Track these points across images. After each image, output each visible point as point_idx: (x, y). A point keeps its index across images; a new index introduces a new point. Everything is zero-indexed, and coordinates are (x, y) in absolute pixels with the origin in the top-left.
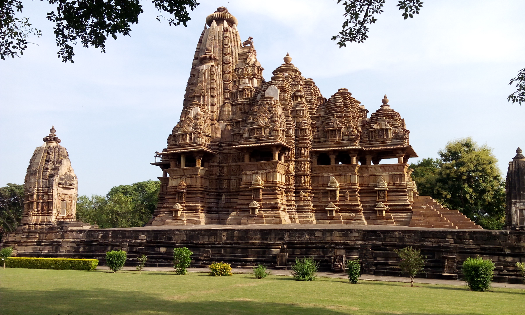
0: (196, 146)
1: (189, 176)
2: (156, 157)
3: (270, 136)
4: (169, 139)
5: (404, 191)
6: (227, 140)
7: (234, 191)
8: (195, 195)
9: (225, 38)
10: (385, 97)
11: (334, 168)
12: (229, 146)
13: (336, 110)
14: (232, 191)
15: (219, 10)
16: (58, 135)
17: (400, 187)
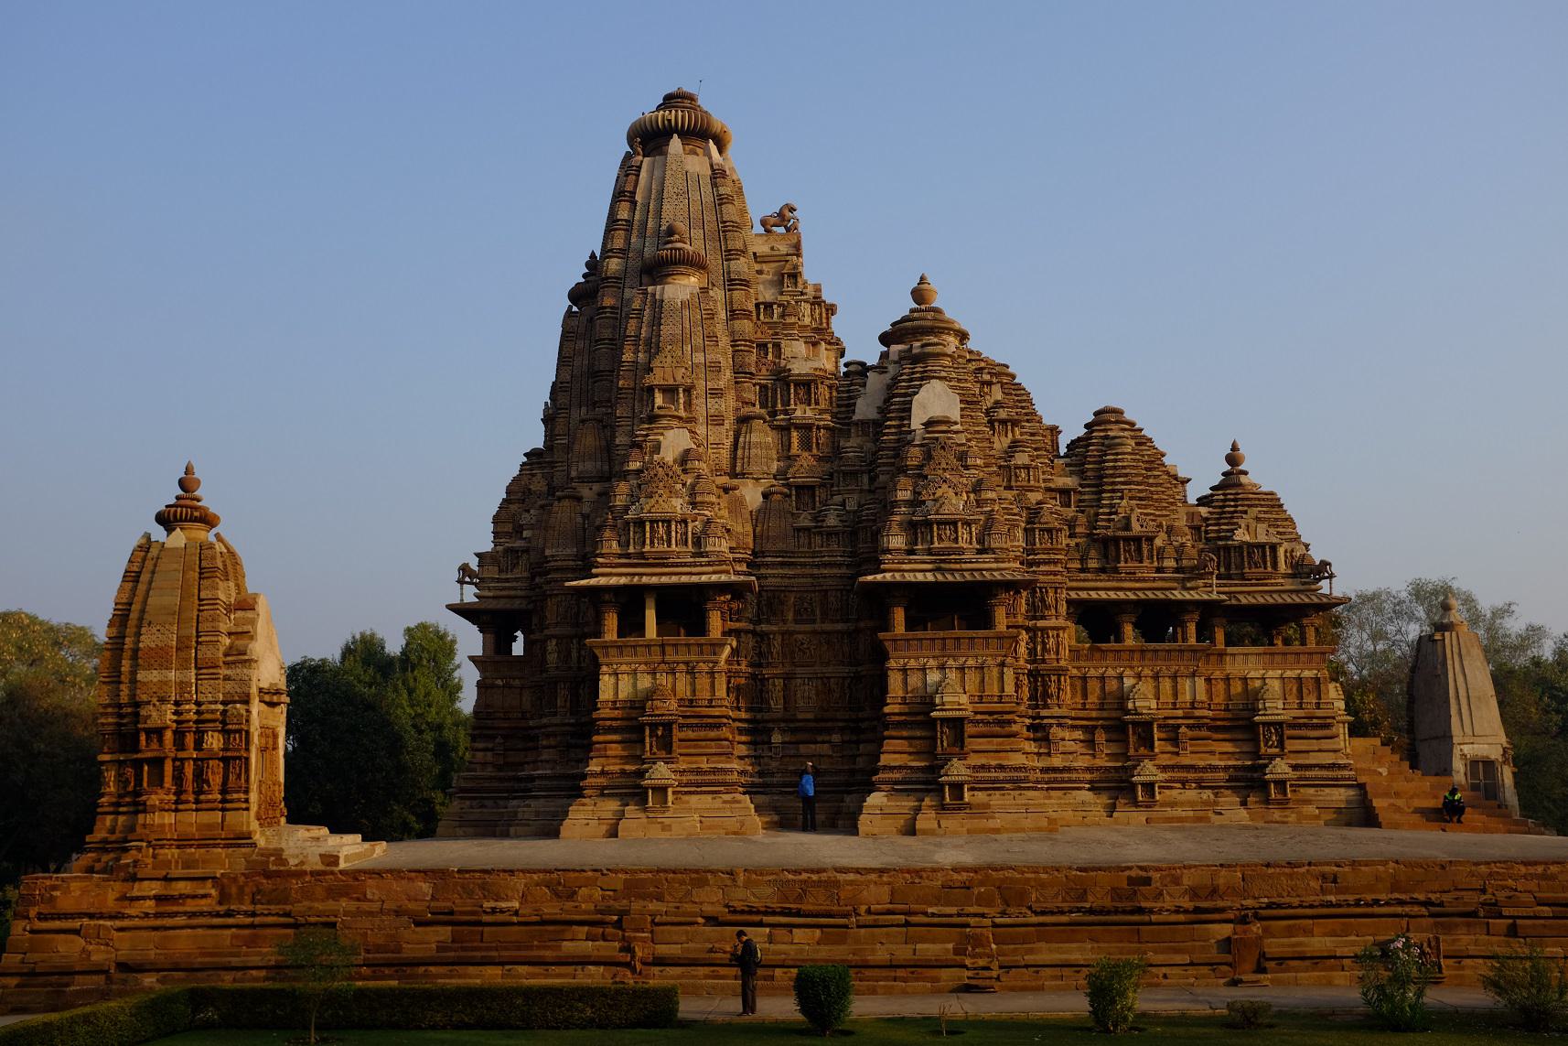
0: (709, 564)
1: (682, 667)
2: (461, 582)
3: (980, 552)
4: (497, 520)
5: (1328, 726)
6: (780, 546)
7: (810, 716)
8: (712, 734)
9: (721, 201)
10: (1234, 448)
11: (1137, 656)
12: (782, 564)
13: (1126, 475)
14: (800, 716)
15: (671, 100)
16: (209, 497)
17: (1319, 713)
